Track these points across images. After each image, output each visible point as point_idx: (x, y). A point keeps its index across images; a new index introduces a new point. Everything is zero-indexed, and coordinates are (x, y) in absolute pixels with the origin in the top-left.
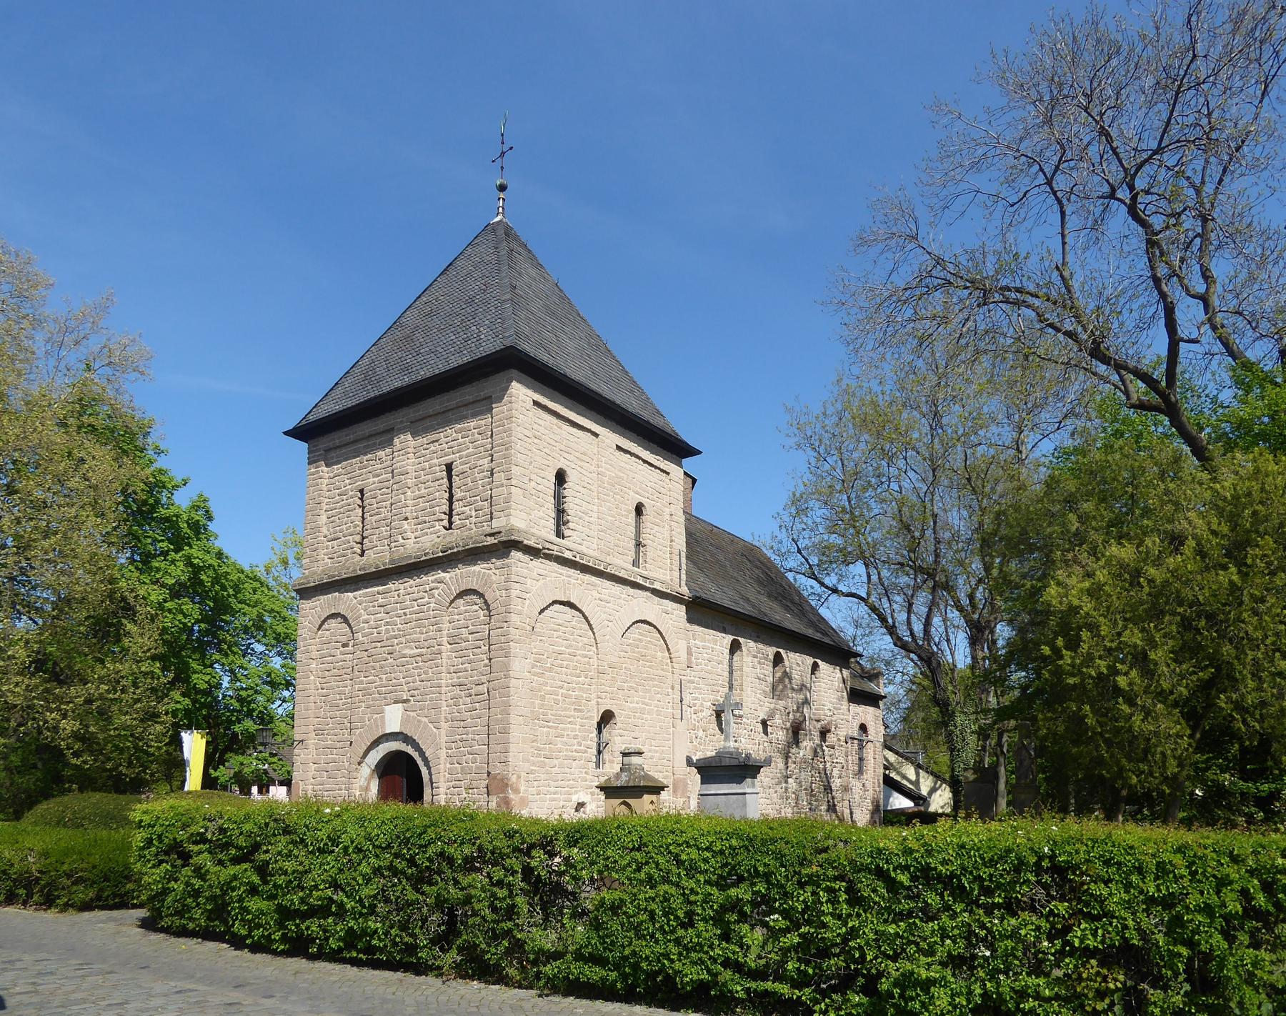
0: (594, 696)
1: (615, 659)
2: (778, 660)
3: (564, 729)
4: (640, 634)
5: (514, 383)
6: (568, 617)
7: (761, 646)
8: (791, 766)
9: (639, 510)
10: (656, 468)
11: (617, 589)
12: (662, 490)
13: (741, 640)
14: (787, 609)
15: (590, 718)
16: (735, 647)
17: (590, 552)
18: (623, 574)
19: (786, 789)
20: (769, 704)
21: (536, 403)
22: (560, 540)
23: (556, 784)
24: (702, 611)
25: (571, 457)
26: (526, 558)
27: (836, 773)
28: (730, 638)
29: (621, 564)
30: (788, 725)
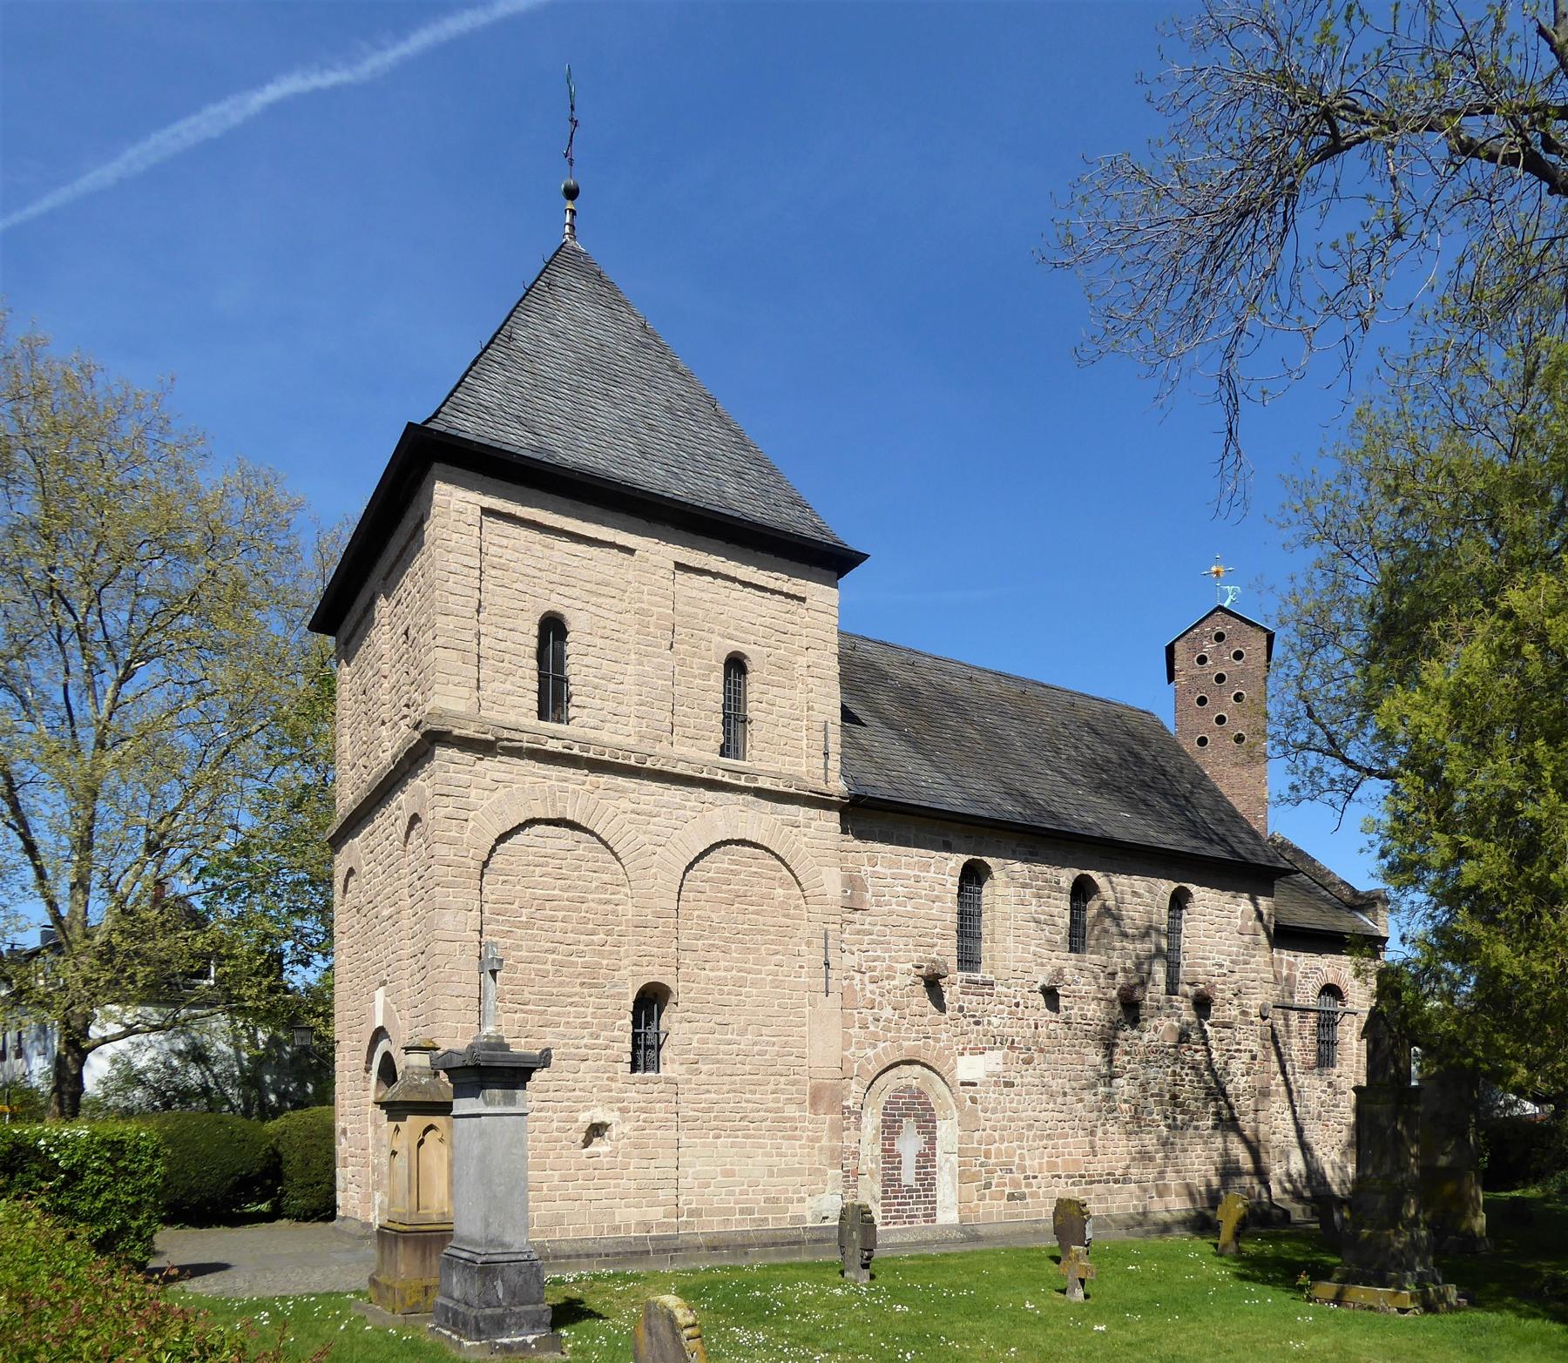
2: (1082, 891)
3: (558, 1015)
4: (733, 862)
5: (440, 487)
6: (570, 843)
7: (1044, 868)
8: (1120, 1059)
9: (736, 665)
10: (773, 592)
11: (675, 794)
12: (791, 628)
13: (988, 860)
14: (1134, 804)
16: (973, 876)
17: (618, 740)
18: (680, 769)
19: (1109, 1097)
20: (1068, 962)
21: (487, 512)
22: (562, 727)
23: (542, 1096)
24: (868, 815)
25: (576, 592)
26: (468, 757)
27: (1236, 1066)
28: (957, 861)
29: (702, 754)
30: (1114, 993)
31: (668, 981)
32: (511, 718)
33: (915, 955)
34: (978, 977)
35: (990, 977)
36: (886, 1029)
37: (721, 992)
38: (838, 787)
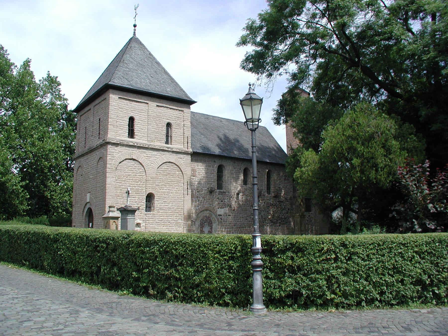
0: (145, 188)
1: (154, 176)
4: (168, 166)
11: (155, 153)
15: (144, 196)
31: (153, 192)
32: (123, 138)
33: (207, 186)
34: (222, 191)
35: (225, 191)
36: (201, 203)
37: (164, 195)
38: (190, 150)
